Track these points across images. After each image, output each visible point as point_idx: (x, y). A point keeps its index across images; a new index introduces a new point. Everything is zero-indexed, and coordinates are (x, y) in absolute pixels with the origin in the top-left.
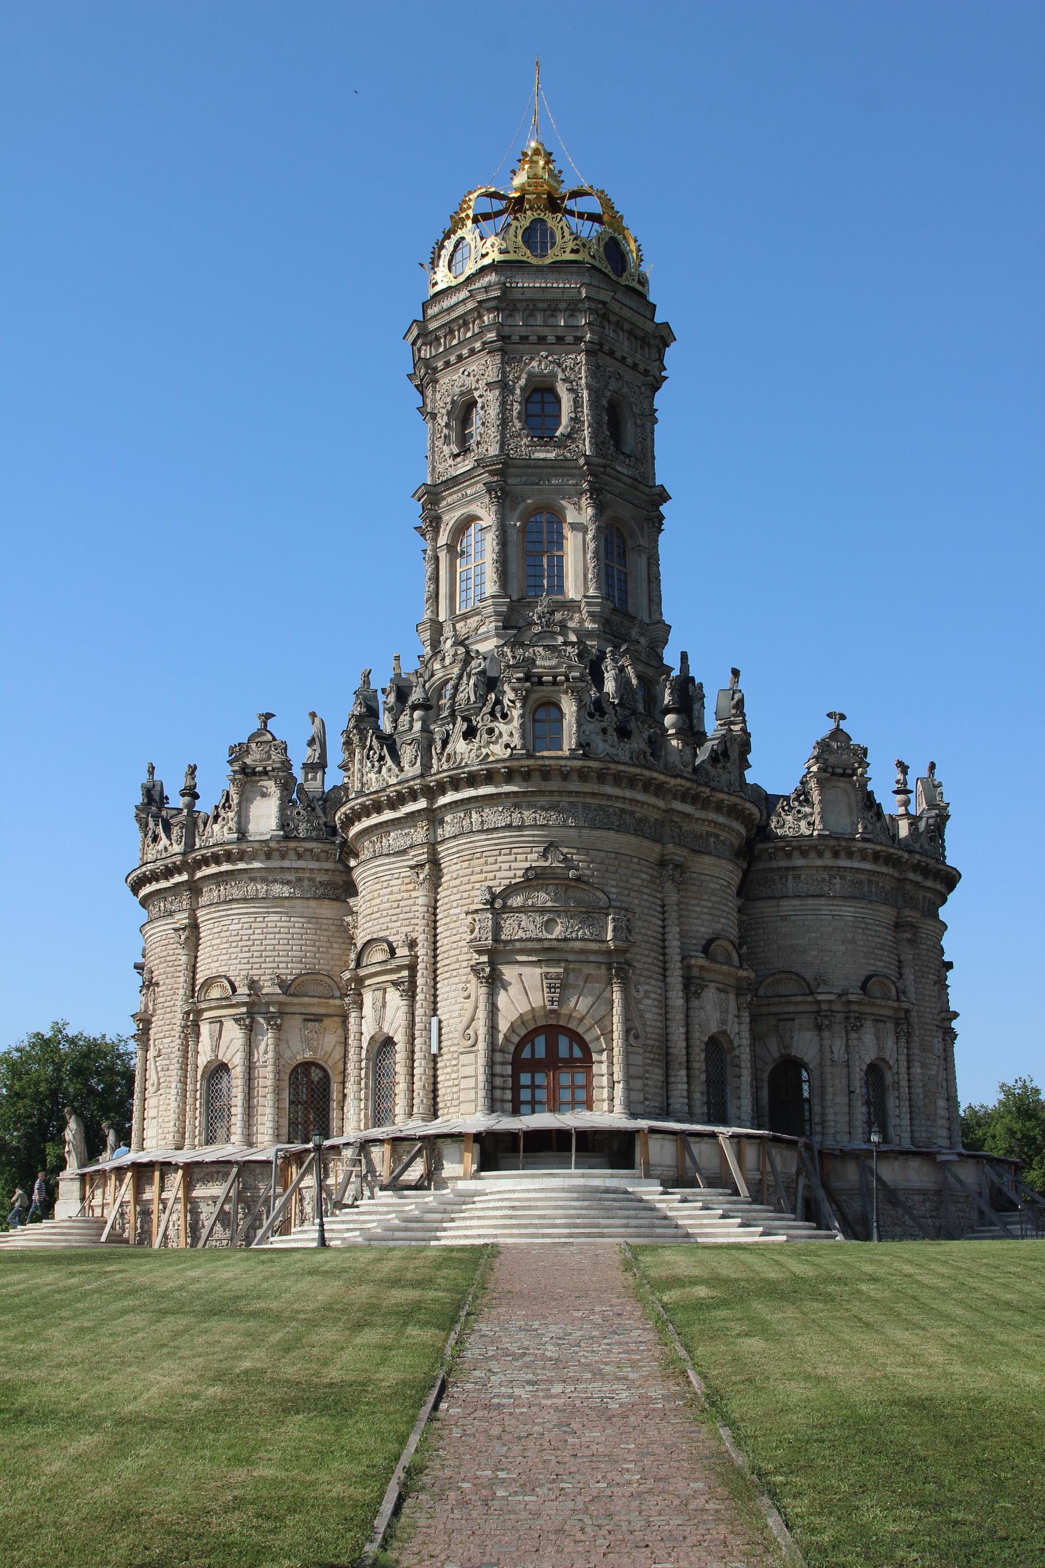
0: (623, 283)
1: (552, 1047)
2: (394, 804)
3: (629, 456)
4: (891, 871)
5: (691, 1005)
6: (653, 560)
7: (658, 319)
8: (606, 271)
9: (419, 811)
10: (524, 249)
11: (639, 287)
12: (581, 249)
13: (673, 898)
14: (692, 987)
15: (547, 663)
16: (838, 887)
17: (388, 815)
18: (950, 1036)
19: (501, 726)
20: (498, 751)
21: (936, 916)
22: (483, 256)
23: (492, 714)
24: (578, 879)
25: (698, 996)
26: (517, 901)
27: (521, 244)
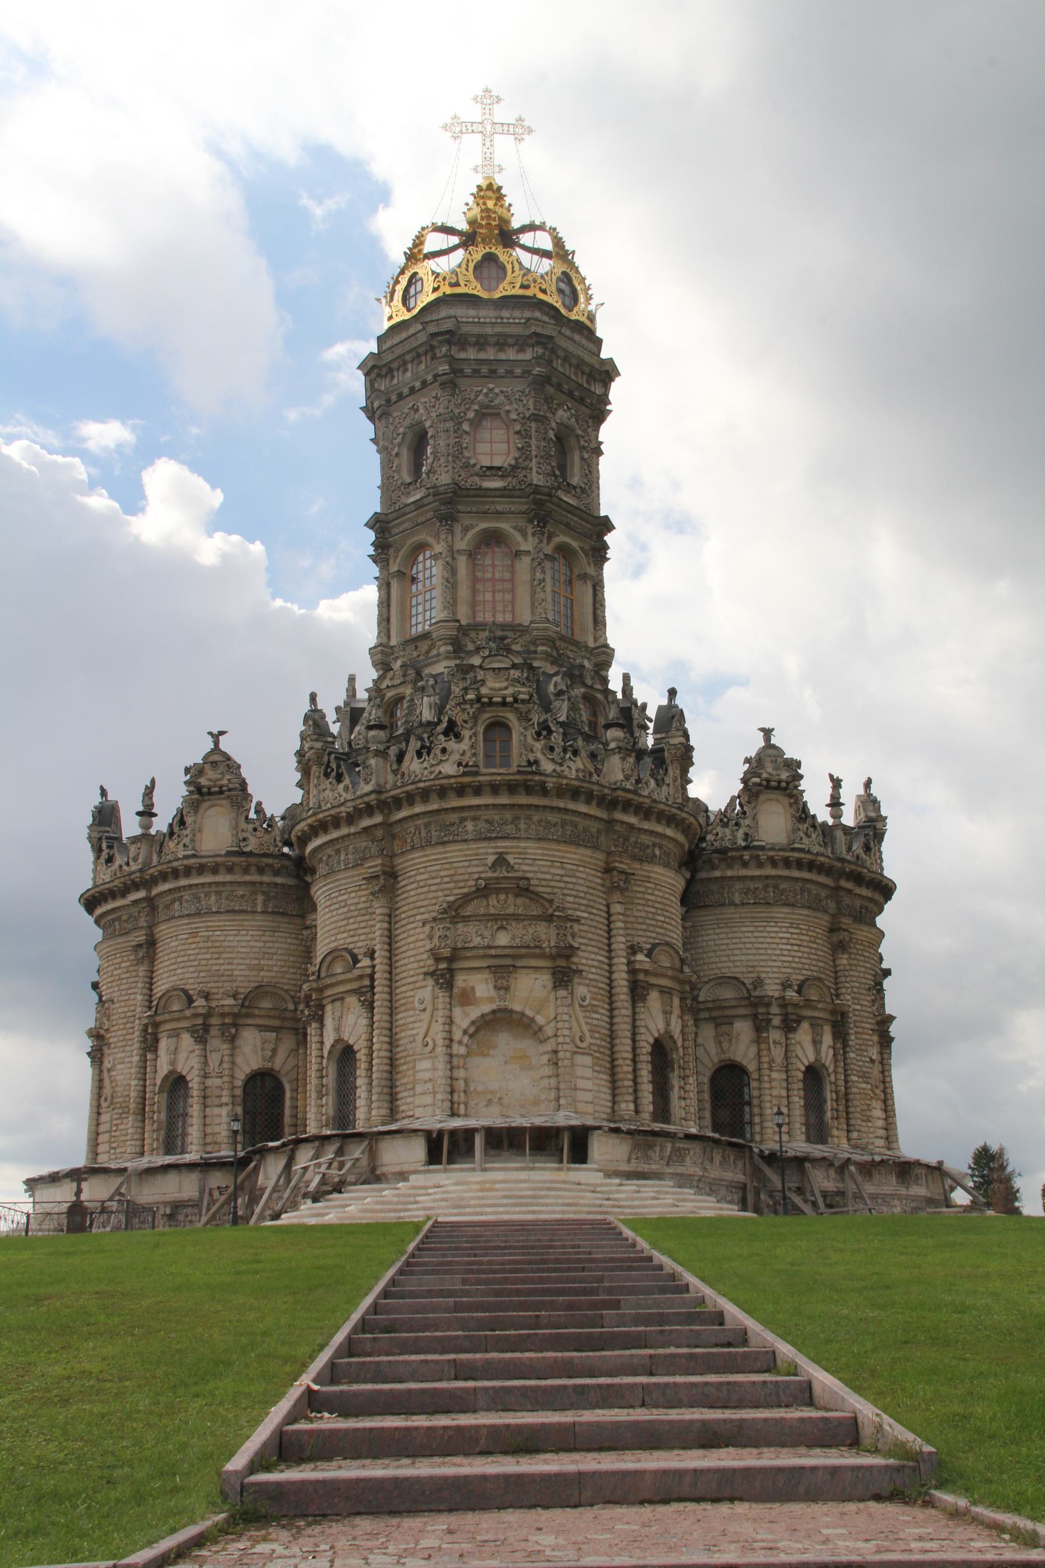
2: (351, 819)
3: (575, 488)
5: (638, 1010)
6: (598, 586)
7: (604, 355)
9: (375, 826)
10: (475, 283)
12: (532, 285)
13: (617, 908)
14: (638, 991)
15: (497, 685)
17: (344, 831)
18: (886, 1041)
19: (452, 745)
20: (449, 768)
21: (874, 925)
24: (527, 890)
25: (644, 999)
27: (472, 277)
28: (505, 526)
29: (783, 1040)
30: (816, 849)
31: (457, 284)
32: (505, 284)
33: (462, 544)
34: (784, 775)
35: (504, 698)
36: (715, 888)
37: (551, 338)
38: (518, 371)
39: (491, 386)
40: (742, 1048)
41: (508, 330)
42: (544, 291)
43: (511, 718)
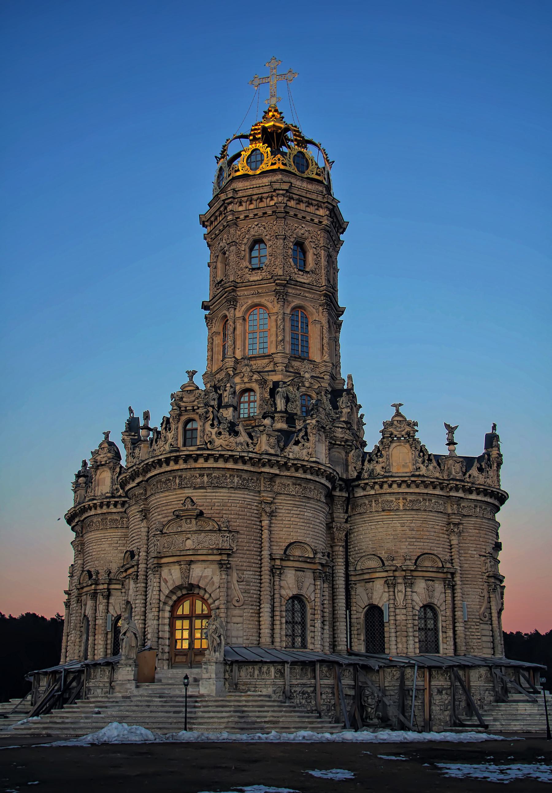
0: (306, 176)
1: (193, 606)
4: (438, 492)
8: (294, 171)
10: (247, 167)
15: (188, 400)
16: (401, 505)
22: (229, 175)
23: (165, 428)
26: (173, 528)
27: (245, 164)
28: (263, 301)
29: (404, 591)
30: (429, 473)
31: (238, 170)
32: (263, 165)
33: (239, 314)
34: (408, 429)
35: (193, 407)
36: (367, 502)
37: (287, 191)
38: (270, 212)
39: (256, 223)
40: (380, 595)
41: (261, 191)
42: (284, 164)
43: (196, 417)
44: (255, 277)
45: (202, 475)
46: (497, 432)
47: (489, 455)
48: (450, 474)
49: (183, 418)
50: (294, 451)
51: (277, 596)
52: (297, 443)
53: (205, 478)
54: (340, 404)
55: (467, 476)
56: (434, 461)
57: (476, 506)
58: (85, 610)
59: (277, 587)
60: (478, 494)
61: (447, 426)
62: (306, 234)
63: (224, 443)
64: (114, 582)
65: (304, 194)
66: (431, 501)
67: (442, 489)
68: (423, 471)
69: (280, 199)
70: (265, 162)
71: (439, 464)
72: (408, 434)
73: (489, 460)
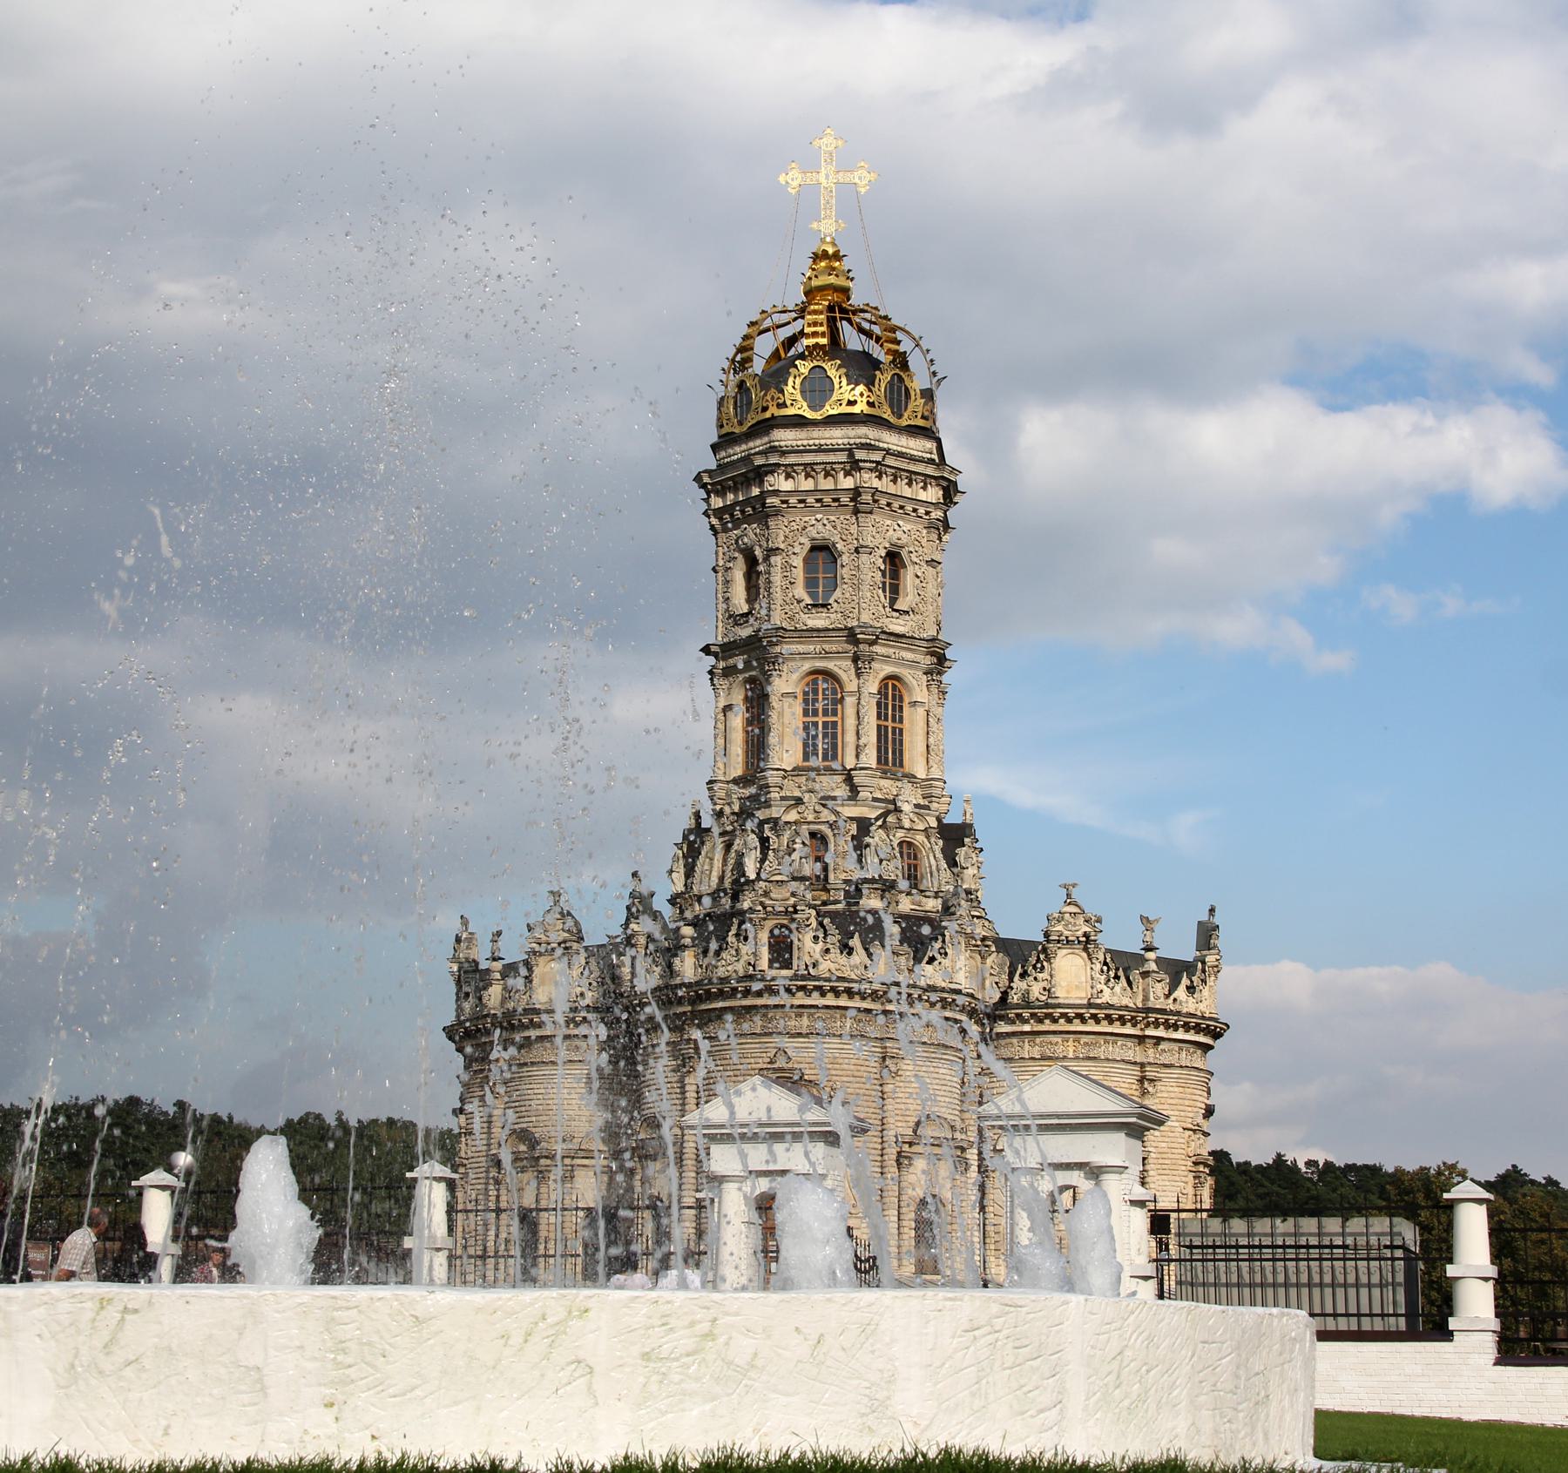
4: (1128, 1030)
11: (921, 423)
16: (1071, 1050)
23: (737, 935)
28: (830, 665)
30: (1114, 1001)
31: (784, 405)
37: (878, 463)
38: (845, 499)
39: (819, 516)
41: (831, 458)
44: (818, 621)
45: (800, 1015)
46: (1217, 920)
47: (1204, 963)
48: (1146, 998)
49: (769, 924)
50: (928, 974)
51: (904, 1197)
52: (932, 960)
53: (805, 1021)
54: (960, 859)
55: (1171, 1000)
56: (1123, 979)
57: (1181, 1049)
58: (520, 1197)
59: (903, 1184)
60: (1187, 1031)
61: (1145, 920)
62: (905, 539)
63: (833, 967)
64: (582, 1154)
65: (904, 466)
66: (1115, 1042)
67: (1134, 1025)
68: (1107, 997)
69: (866, 476)
70: (834, 398)
71: (1130, 983)
72: (1086, 935)
73: (1204, 971)
